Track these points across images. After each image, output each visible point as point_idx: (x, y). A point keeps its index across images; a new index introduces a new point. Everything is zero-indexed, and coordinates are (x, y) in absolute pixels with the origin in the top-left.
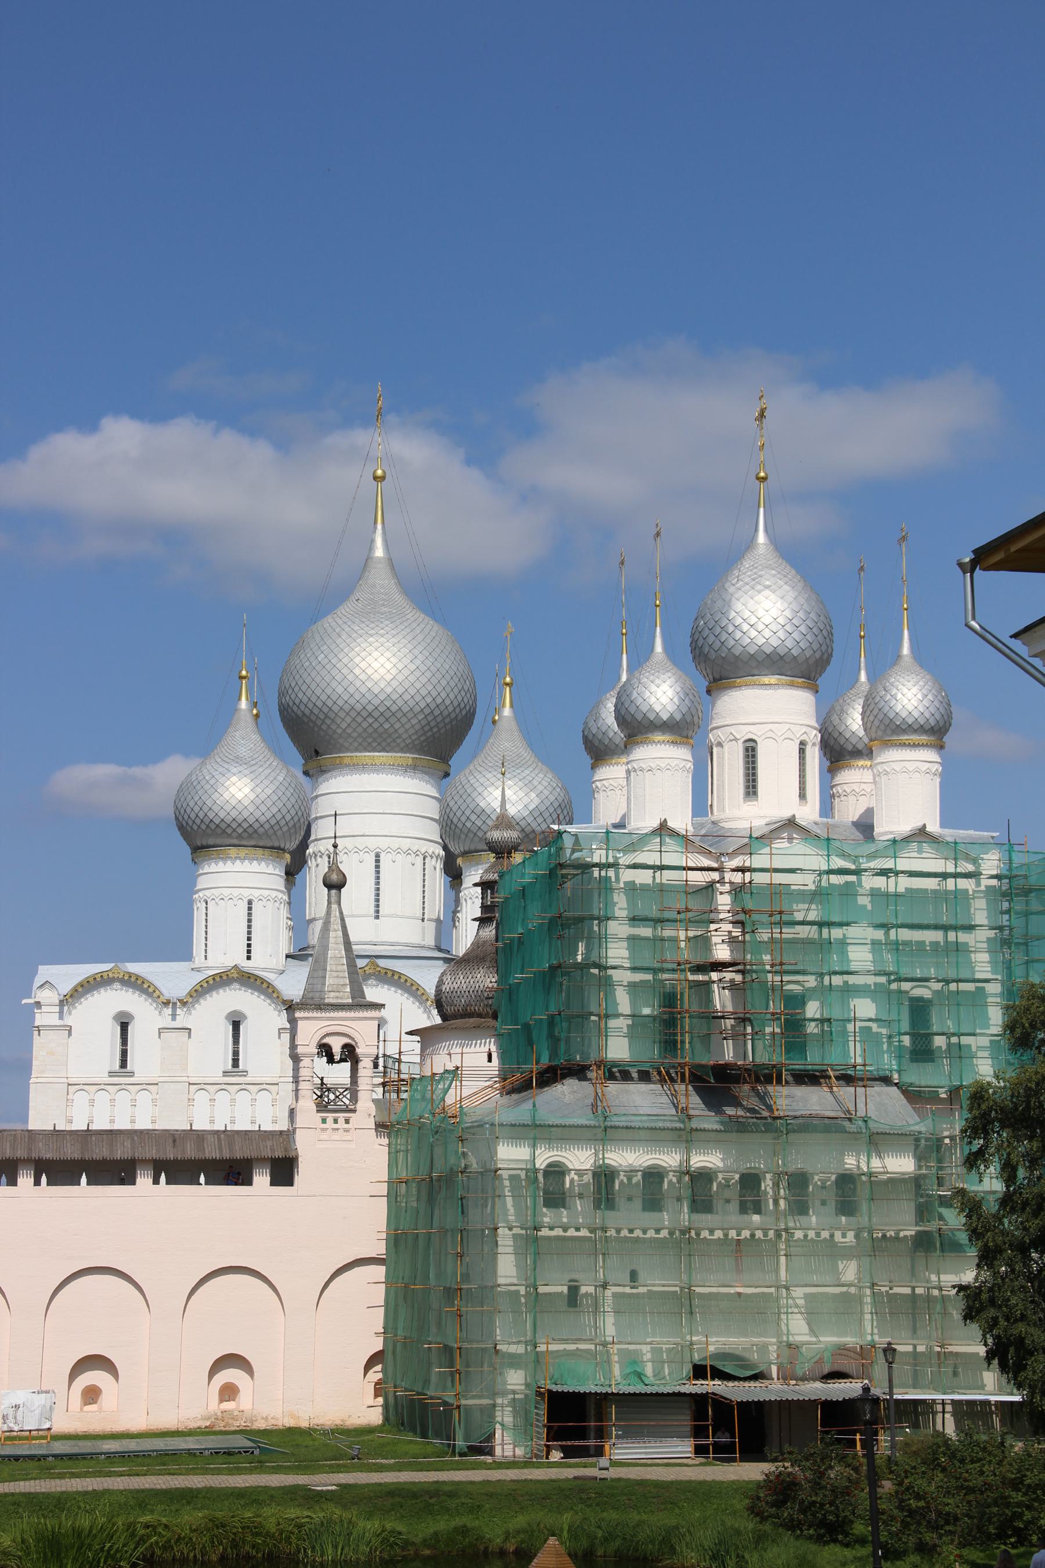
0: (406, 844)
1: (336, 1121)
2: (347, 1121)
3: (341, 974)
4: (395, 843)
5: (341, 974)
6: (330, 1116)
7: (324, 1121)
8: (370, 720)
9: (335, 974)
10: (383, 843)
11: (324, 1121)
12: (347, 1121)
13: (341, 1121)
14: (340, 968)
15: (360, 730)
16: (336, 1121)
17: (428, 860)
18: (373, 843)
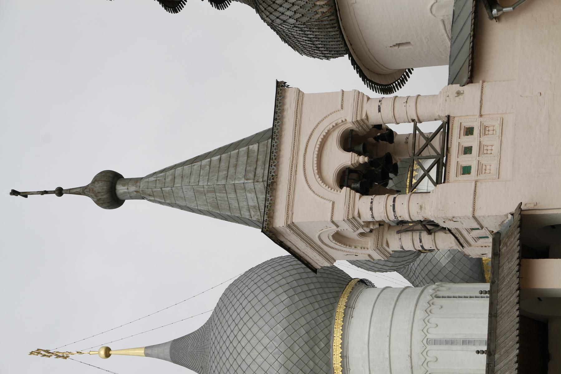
0: (420, 314)
1: (468, 150)
2: (469, 131)
3: (233, 161)
4: (418, 325)
5: (233, 161)
6: (456, 159)
7: (466, 170)
8: (296, 348)
9: (232, 170)
10: (418, 336)
11: (466, 170)
12: (469, 131)
13: (467, 141)
14: (223, 165)
15: (306, 359)
16: (468, 150)
17: (440, 294)
18: (417, 348)
